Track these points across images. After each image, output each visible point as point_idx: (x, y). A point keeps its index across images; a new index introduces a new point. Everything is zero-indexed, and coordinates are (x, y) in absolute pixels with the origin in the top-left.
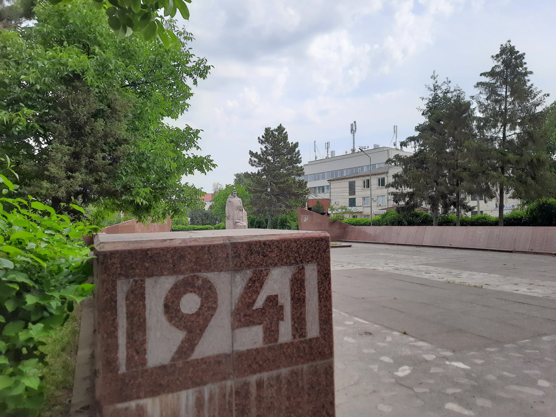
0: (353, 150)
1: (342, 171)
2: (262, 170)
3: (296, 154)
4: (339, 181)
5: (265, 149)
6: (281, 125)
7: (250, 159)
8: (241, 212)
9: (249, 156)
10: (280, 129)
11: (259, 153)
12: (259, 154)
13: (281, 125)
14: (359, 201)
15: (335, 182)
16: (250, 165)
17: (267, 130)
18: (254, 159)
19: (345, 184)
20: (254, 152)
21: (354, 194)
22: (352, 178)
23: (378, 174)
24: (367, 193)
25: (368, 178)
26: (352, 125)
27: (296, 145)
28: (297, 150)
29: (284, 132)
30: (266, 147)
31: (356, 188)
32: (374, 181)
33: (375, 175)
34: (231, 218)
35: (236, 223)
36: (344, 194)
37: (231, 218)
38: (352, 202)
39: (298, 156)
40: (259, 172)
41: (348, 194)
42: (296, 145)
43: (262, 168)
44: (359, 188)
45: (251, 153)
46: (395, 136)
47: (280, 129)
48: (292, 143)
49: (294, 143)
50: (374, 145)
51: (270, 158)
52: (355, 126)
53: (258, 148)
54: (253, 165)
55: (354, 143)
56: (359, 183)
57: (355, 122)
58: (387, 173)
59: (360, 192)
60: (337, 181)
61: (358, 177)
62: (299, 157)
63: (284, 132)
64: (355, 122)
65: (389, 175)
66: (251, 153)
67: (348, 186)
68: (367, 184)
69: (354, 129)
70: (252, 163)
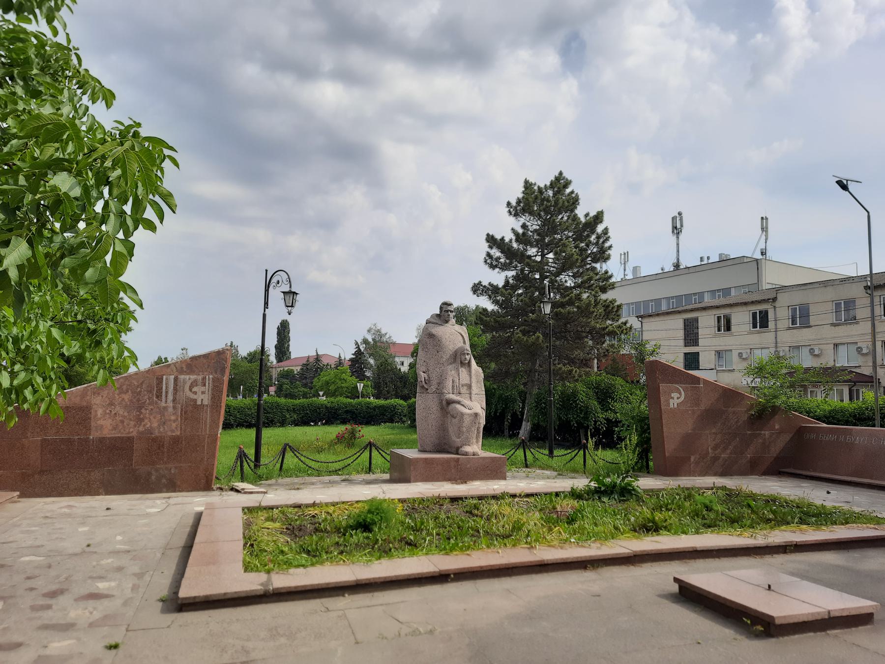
0: (677, 266)
1: (658, 301)
2: (515, 278)
3: (598, 237)
4: (662, 318)
5: (521, 231)
6: (561, 173)
7: (489, 255)
8: (463, 371)
9: (485, 247)
10: (560, 183)
11: (509, 236)
12: (507, 240)
13: (561, 173)
14: (706, 359)
15: (652, 319)
16: (487, 267)
17: (528, 185)
18: (496, 253)
19: (676, 324)
20: (498, 237)
21: (696, 343)
22: (692, 310)
23: (753, 302)
24: (725, 341)
25: (727, 311)
26: (674, 219)
27: (598, 218)
28: (600, 229)
29: (568, 191)
30: (524, 226)
31: (700, 331)
32: (741, 318)
33: (745, 304)
34: (433, 388)
35: (450, 402)
36: (673, 343)
37: (433, 388)
38: (692, 361)
39: (604, 242)
40: (507, 282)
41: (682, 342)
42: (598, 218)
43: (513, 273)
44: (707, 331)
45: (491, 240)
46: (764, 237)
47: (560, 183)
48: (587, 215)
49: (592, 214)
50: (720, 255)
51: (532, 251)
52: (681, 220)
53: (507, 227)
54: (492, 267)
55: (678, 251)
56: (707, 323)
57: (680, 214)
58: (775, 300)
59: (709, 340)
60: (657, 319)
61: (704, 309)
62: (607, 245)
63: (568, 191)
64: (680, 214)
65: (777, 304)
66: (491, 240)
67: (681, 325)
68: (726, 325)
69: (678, 226)
70: (492, 263)
